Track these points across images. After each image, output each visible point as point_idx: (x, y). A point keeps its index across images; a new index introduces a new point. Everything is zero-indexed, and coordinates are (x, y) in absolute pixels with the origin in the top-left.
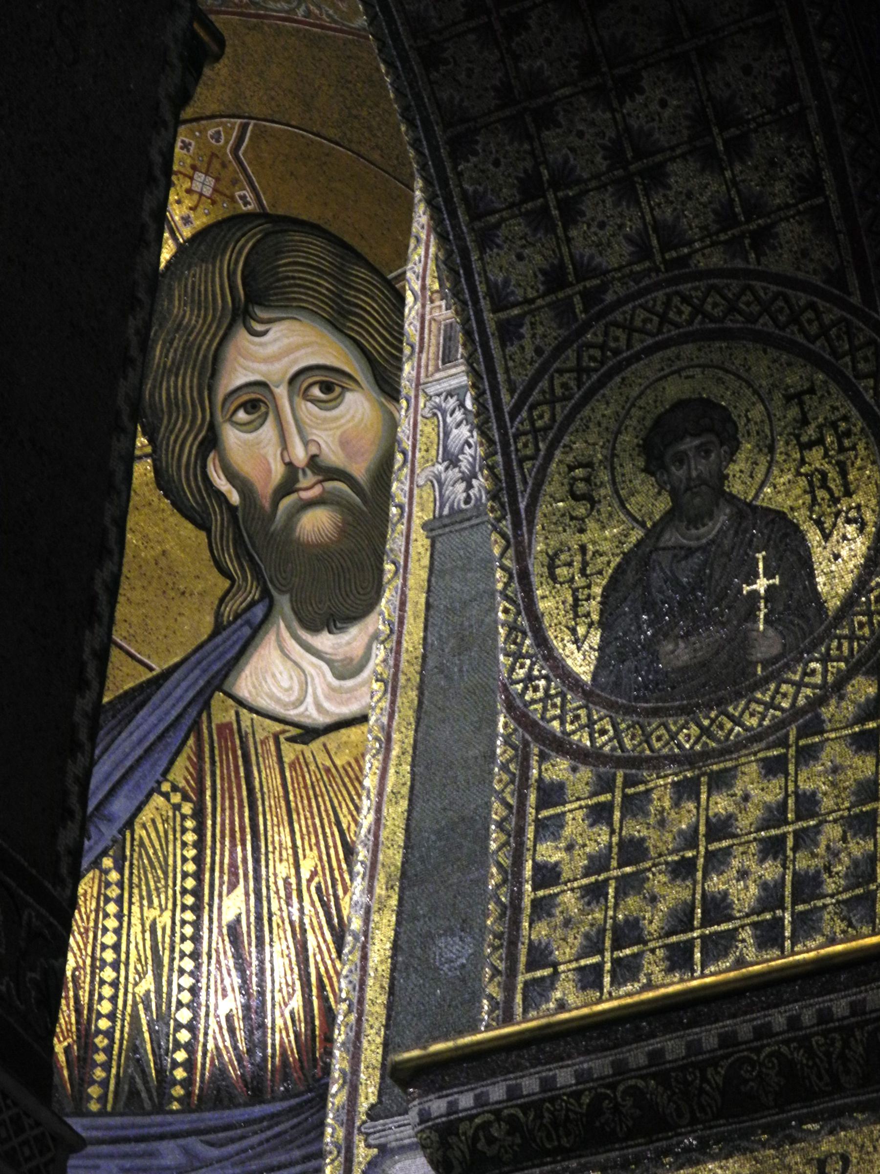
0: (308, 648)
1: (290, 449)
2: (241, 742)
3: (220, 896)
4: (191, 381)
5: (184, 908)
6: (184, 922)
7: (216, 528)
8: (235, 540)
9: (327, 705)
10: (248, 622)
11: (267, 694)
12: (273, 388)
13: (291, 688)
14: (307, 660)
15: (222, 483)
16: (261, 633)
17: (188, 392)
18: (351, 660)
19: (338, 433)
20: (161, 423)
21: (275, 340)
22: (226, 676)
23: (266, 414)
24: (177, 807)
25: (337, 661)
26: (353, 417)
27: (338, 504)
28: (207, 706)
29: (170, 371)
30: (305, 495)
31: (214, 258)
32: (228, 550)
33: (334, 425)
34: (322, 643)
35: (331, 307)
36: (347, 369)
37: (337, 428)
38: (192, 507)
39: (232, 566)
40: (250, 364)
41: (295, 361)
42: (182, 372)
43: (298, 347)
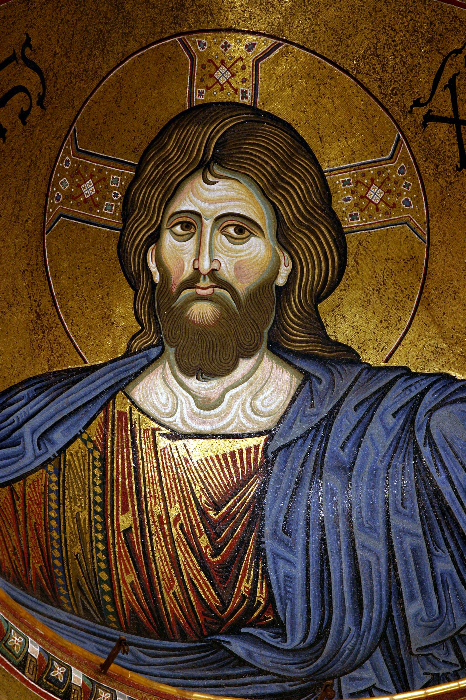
0: (182, 385)
1: (200, 259)
2: (131, 426)
3: (117, 514)
4: (158, 195)
5: (96, 513)
6: (96, 522)
7: (141, 291)
8: (149, 303)
9: (189, 422)
10: (146, 356)
11: (150, 403)
12: (203, 218)
13: (166, 405)
14: (180, 391)
15: (153, 266)
16: (153, 365)
17: (154, 200)
18: (210, 399)
19: (236, 260)
20: (133, 213)
21: (218, 190)
22: (127, 384)
23: (194, 234)
24: (91, 451)
25: (200, 397)
26: (251, 253)
27: (220, 303)
28: (113, 397)
29: (150, 184)
30: (200, 292)
31: (205, 125)
32: (144, 308)
33: (235, 255)
34: (191, 384)
35: (268, 180)
36: (259, 222)
37: (237, 257)
38: (132, 274)
39: (144, 319)
40: (195, 199)
41: (225, 208)
42: (156, 186)
43: (231, 199)
